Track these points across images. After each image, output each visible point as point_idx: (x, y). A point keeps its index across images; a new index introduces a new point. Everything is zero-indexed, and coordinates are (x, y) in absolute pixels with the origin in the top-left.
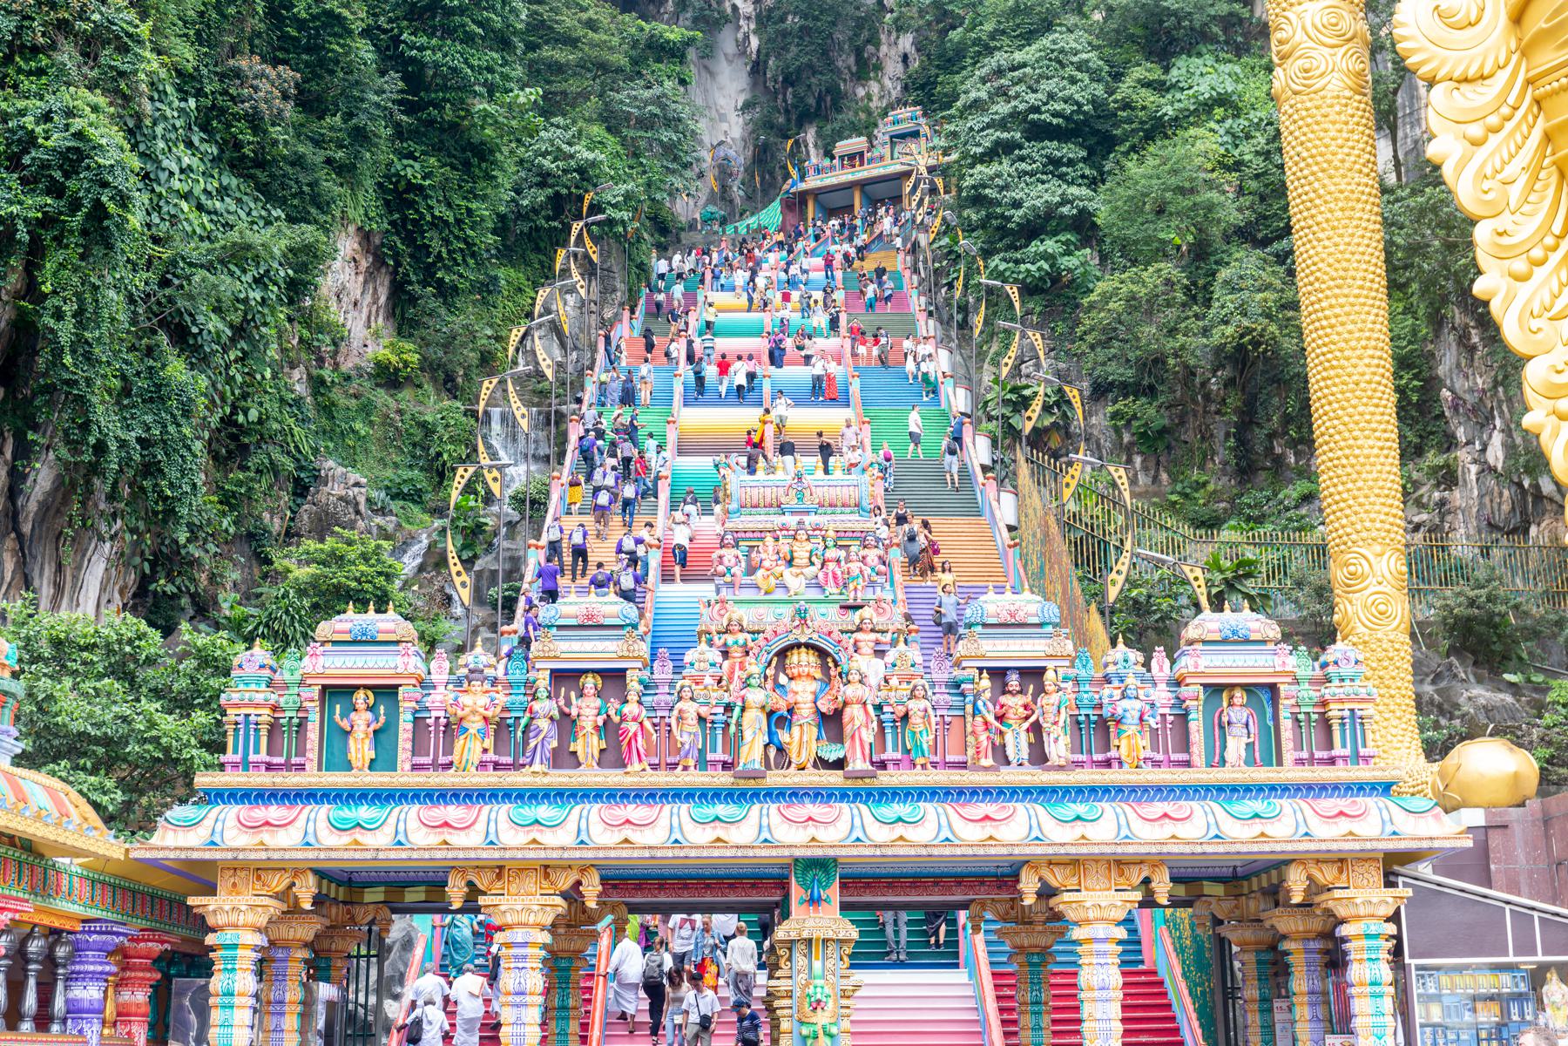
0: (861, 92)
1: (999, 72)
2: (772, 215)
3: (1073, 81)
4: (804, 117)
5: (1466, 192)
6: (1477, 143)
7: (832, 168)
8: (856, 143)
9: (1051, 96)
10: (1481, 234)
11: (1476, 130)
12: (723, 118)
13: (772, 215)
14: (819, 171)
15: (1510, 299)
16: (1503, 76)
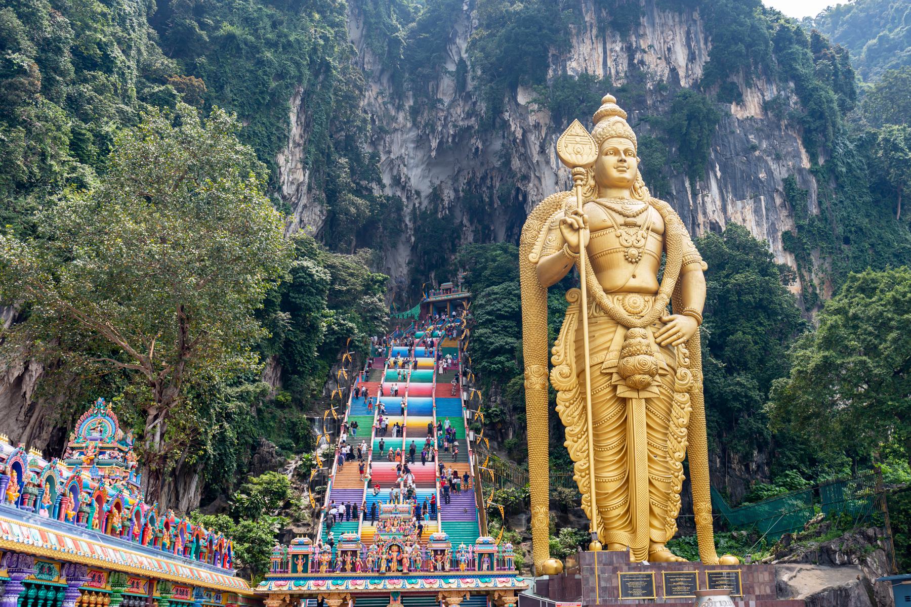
0: (453, 257)
1: (489, 295)
2: (416, 310)
3: (512, 300)
4: (431, 267)
5: (564, 420)
6: (568, 407)
7: (439, 294)
8: (448, 285)
9: (505, 305)
10: (567, 430)
11: (567, 404)
12: (400, 266)
13: (416, 310)
14: (434, 294)
15: (572, 447)
16: (574, 390)
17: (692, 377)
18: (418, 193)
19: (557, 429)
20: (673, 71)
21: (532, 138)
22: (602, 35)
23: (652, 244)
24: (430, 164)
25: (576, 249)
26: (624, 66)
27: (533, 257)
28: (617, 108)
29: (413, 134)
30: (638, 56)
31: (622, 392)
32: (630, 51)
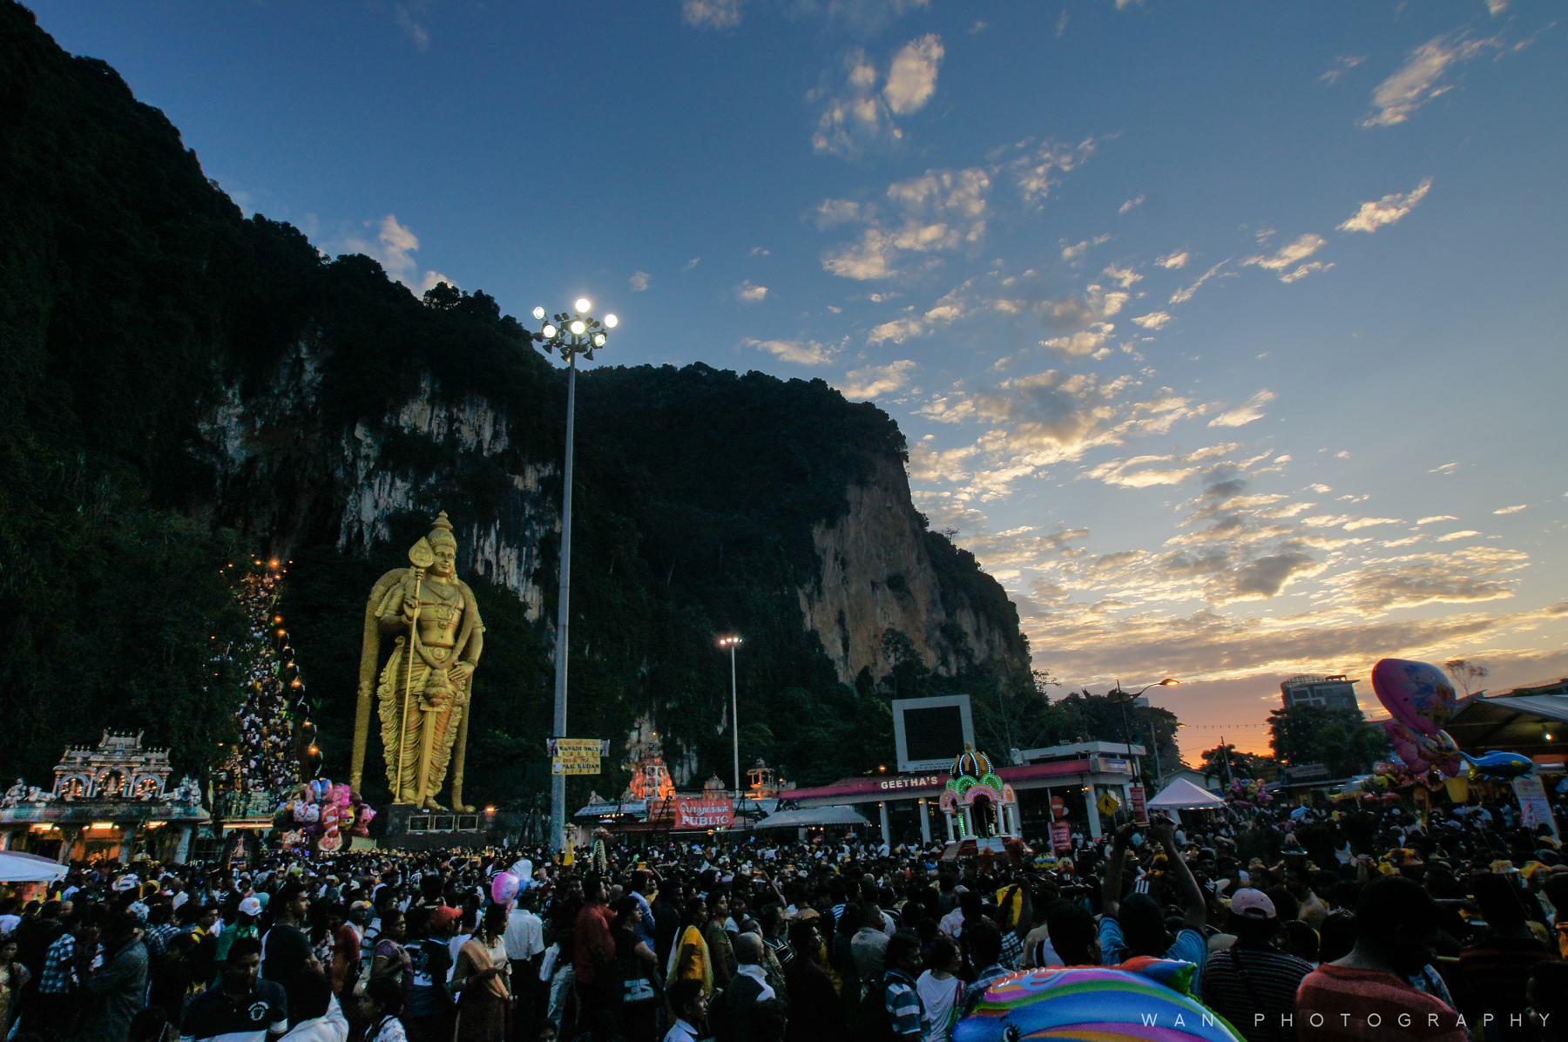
17: (465, 698)
18: (233, 461)
19: (375, 725)
20: (480, 443)
21: (361, 464)
22: (432, 402)
23: (455, 617)
24: (249, 439)
25: (410, 619)
26: (444, 430)
27: (377, 614)
28: (447, 523)
29: (240, 410)
30: (456, 425)
31: (423, 707)
32: (451, 420)
